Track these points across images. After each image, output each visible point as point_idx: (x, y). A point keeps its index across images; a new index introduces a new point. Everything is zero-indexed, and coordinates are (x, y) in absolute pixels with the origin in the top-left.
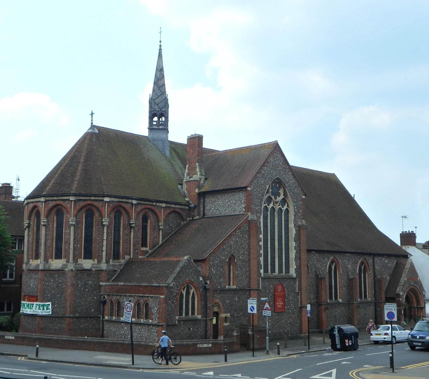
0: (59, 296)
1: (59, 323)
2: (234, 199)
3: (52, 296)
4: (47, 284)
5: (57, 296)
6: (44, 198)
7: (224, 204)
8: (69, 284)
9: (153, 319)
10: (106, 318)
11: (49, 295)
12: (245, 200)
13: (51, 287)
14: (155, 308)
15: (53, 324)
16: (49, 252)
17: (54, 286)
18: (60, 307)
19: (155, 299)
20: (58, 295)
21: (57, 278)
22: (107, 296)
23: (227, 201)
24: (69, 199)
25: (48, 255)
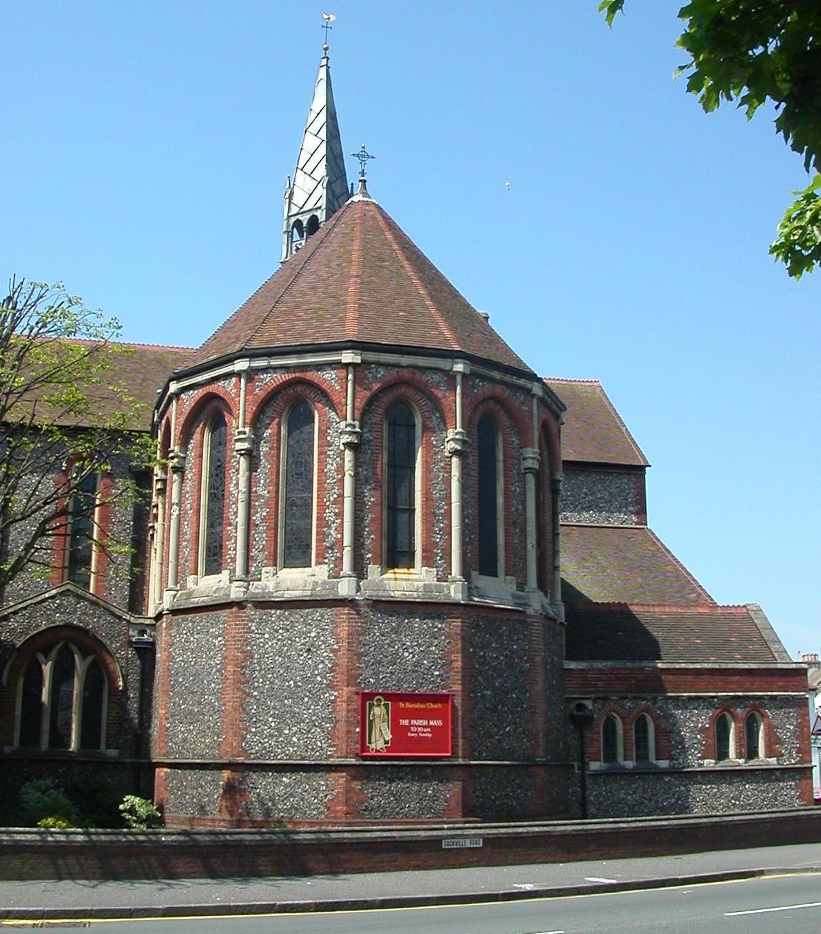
0: (514, 696)
1: (520, 787)
2: (605, 490)
3: (495, 697)
4: (482, 654)
5: (509, 696)
6: (467, 362)
7: (574, 496)
8: (538, 659)
9: (783, 755)
10: (595, 766)
11: (489, 692)
12: (636, 496)
13: (494, 664)
14: (788, 726)
15: (504, 790)
16: (469, 547)
17: (501, 661)
18: (519, 733)
19: (785, 703)
20: (511, 694)
21: (507, 636)
22: (594, 703)
23: (586, 491)
24: (531, 390)
25: (469, 555)
